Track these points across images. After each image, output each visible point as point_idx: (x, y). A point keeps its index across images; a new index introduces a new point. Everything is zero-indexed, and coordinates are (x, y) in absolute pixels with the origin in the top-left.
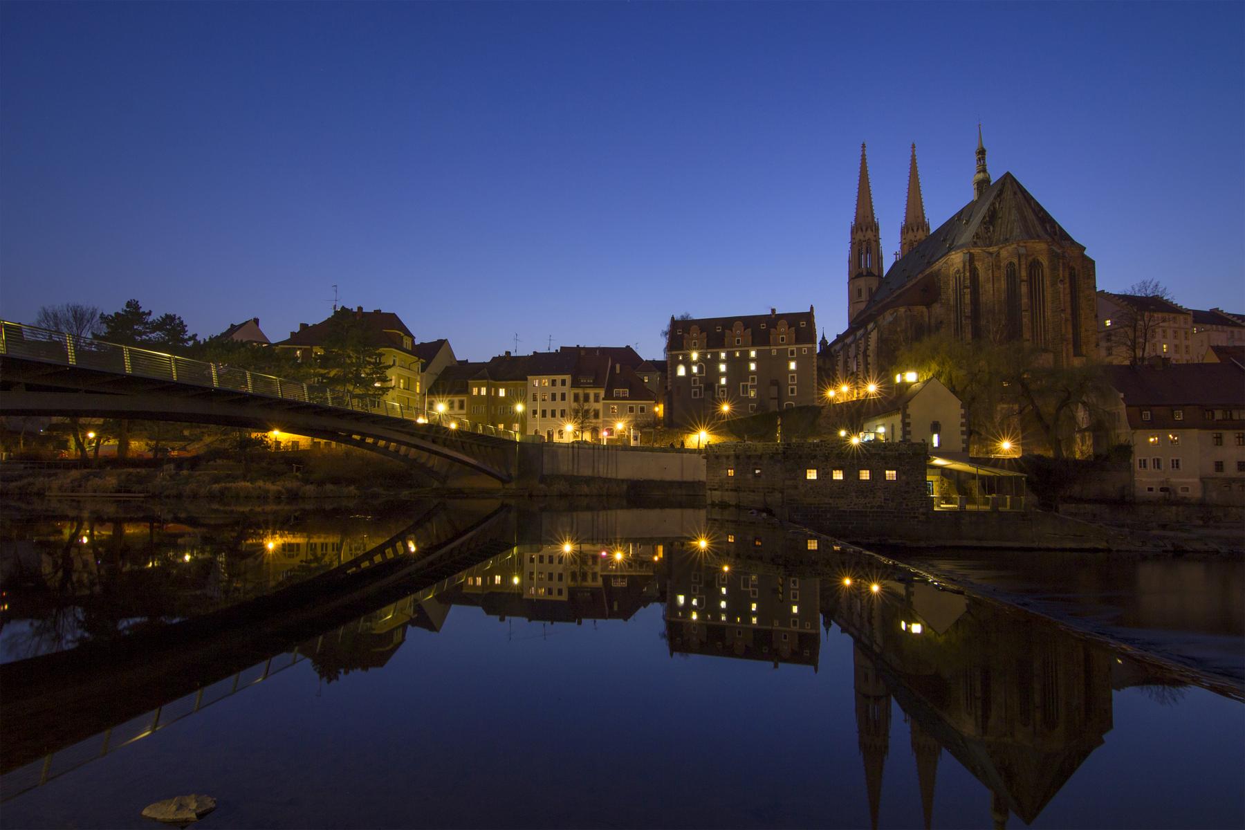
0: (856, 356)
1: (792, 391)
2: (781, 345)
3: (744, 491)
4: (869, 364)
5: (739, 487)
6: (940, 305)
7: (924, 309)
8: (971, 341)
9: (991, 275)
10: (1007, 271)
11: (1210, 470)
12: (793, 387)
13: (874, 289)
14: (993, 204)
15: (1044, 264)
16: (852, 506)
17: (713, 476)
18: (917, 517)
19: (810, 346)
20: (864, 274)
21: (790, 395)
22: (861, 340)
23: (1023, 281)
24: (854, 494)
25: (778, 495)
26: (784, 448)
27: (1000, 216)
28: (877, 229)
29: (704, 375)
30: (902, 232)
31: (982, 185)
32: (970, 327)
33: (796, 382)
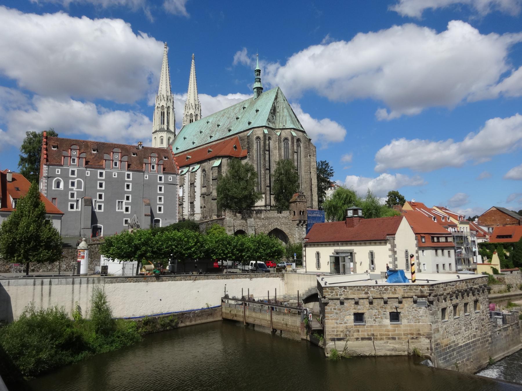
1: (160, 209)
3: (381, 339)
5: (373, 335)
9: (277, 146)
10: (284, 144)
13: (171, 141)
14: (274, 103)
15: (301, 144)
16: (464, 340)
17: (337, 323)
23: (295, 152)
26: (430, 290)
32: (269, 175)
33: (163, 203)
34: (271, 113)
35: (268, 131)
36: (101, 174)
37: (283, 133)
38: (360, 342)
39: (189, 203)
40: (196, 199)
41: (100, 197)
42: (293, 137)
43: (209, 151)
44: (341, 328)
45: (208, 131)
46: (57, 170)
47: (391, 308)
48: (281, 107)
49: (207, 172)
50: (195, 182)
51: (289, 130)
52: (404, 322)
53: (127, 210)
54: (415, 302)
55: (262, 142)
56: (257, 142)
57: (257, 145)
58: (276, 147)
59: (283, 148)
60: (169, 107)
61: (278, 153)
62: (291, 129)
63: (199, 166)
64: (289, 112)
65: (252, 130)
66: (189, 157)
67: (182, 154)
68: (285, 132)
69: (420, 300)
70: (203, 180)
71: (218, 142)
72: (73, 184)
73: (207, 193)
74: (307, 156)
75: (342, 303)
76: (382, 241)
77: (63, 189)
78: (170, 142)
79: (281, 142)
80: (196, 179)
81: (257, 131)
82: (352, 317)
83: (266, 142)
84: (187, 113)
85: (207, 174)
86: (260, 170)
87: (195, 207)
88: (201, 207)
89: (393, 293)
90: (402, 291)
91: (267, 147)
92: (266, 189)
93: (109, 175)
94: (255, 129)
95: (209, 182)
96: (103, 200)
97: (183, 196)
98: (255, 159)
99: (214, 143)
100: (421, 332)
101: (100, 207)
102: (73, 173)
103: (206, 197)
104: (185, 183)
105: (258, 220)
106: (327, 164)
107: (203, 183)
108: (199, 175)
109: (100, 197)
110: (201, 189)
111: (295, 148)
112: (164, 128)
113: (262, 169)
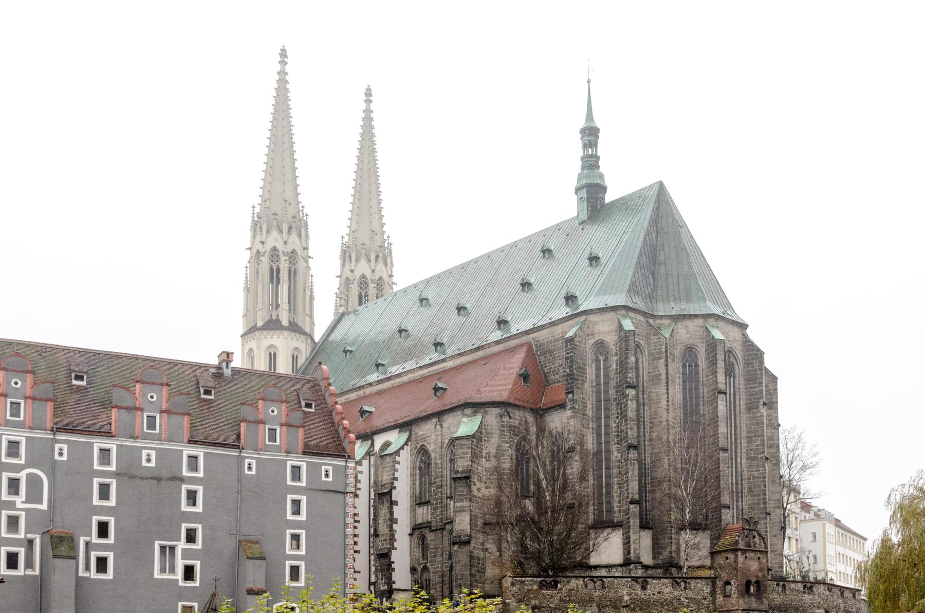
4: (392, 520)
6: (569, 413)
7: (530, 418)
8: (637, 497)
9: (663, 372)
10: (684, 366)
13: (301, 361)
15: (736, 367)
20: (285, 323)
22: (361, 465)
23: (720, 393)
30: (344, 253)
32: (637, 466)
35: (633, 323)
37: (680, 331)
39: (372, 557)
40: (396, 545)
42: (712, 345)
43: (436, 389)
49: (433, 455)
50: (395, 488)
51: (699, 322)
55: (615, 358)
56: (597, 360)
57: (598, 369)
58: (660, 375)
61: (665, 396)
63: (405, 436)
65: (583, 318)
70: (418, 482)
71: (463, 360)
73: (433, 524)
74: (758, 407)
78: (299, 365)
79: (673, 360)
80: (396, 479)
81: (596, 323)
83: (627, 358)
84: (349, 275)
85: (433, 461)
86: (608, 451)
87: (393, 570)
88: (413, 570)
91: (631, 375)
92: (627, 512)
94: (591, 318)
95: (441, 487)
96: (111, 540)
98: (589, 413)
103: (430, 536)
104: (358, 492)
107: (418, 493)
108: (405, 462)
111: (721, 378)
113: (614, 448)
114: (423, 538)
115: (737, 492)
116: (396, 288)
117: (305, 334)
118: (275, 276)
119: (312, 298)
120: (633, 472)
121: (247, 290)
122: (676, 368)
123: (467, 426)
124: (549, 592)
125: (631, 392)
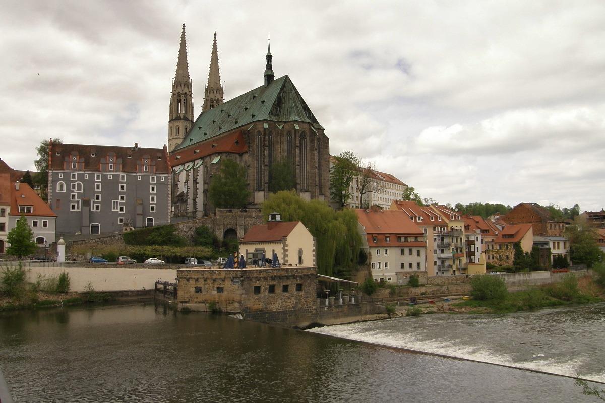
0: (186, 182)
2: (144, 172)
4: (198, 189)
6: (248, 154)
7: (238, 156)
11: (400, 270)
12: (152, 202)
14: (279, 94)
18: (312, 312)
19: (166, 175)
20: (182, 117)
21: (151, 211)
24: (280, 301)
25: (237, 305)
27: (284, 102)
28: (191, 87)
29: (82, 192)
30: (206, 90)
31: (269, 77)
32: (268, 171)
34: (274, 105)
36: (98, 176)
38: (197, 305)
41: (98, 198)
42: (296, 131)
43: (213, 146)
44: (187, 296)
45: (220, 122)
46: (60, 174)
47: (218, 284)
48: (288, 97)
51: (292, 123)
52: (225, 292)
53: (122, 209)
54: (232, 280)
59: (285, 143)
60: (186, 93)
62: (295, 122)
64: (295, 102)
66: (196, 151)
67: (194, 146)
68: (288, 125)
69: (236, 280)
72: (74, 187)
75: (188, 280)
76: (278, 241)
77: (65, 191)
79: (284, 136)
82: (194, 289)
86: (261, 167)
88: (204, 204)
89: (219, 275)
90: (225, 274)
93: (105, 177)
94: (257, 124)
97: (187, 193)
99: (222, 136)
100: (235, 300)
101: (97, 207)
102: (74, 176)
105: (248, 219)
106: (352, 154)
108: (201, 170)
109: (98, 198)
110: (204, 185)
111: (298, 142)
112: (180, 116)
113: (262, 165)
114: (206, 194)
115: (306, 178)
116: (224, 102)
117: (189, 121)
118: (179, 101)
119: (193, 108)
120: (267, 173)
121: (170, 107)
122: (285, 139)
123: (216, 160)
124: (229, 213)
125: (267, 148)
